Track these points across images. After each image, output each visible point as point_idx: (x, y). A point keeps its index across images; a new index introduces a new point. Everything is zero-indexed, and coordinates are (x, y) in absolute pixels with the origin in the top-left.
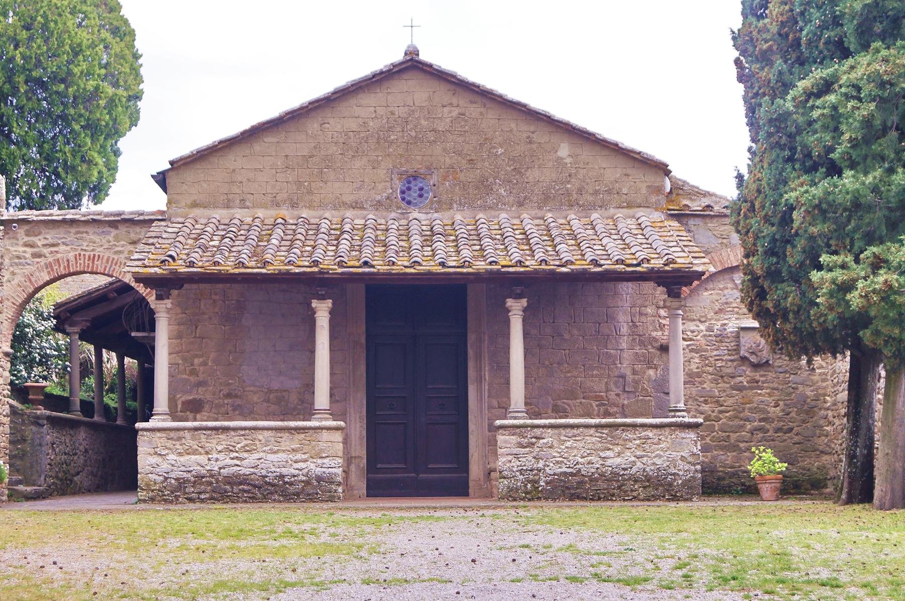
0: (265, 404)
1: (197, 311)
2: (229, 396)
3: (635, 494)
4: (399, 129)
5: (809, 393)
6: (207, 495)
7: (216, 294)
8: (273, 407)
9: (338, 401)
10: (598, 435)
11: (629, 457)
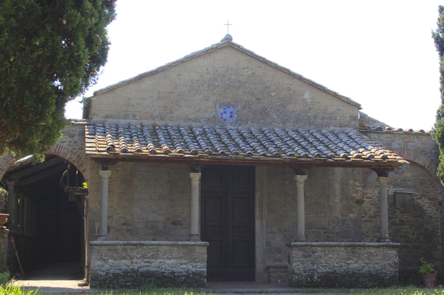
2: (125, 224)
3: (364, 284)
4: (220, 79)
5: (429, 228)
6: (131, 283)
9: (185, 228)
10: (345, 251)
11: (361, 263)
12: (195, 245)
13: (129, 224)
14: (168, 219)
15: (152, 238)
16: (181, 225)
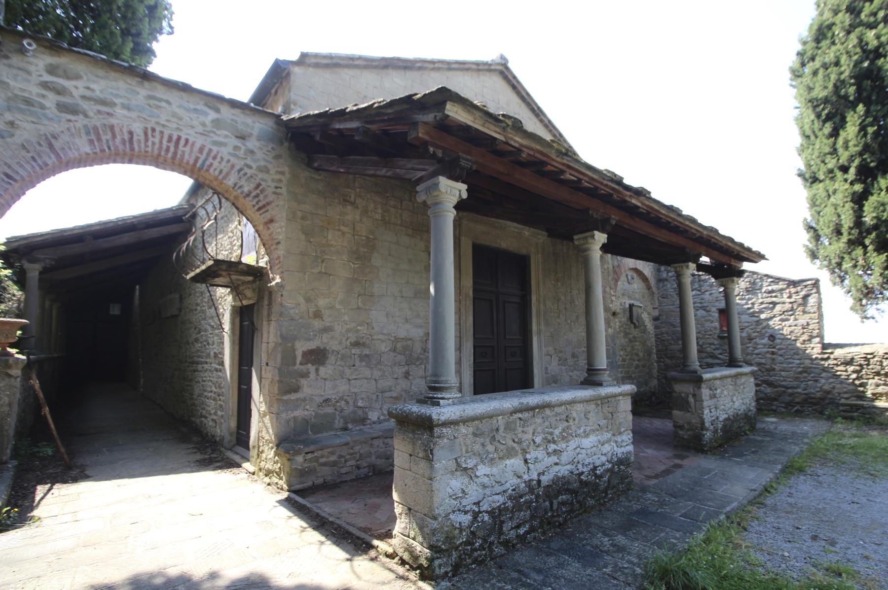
0: (392, 354)
1: (324, 241)
2: (356, 344)
8: (400, 358)
13: (364, 345)
15: (404, 370)
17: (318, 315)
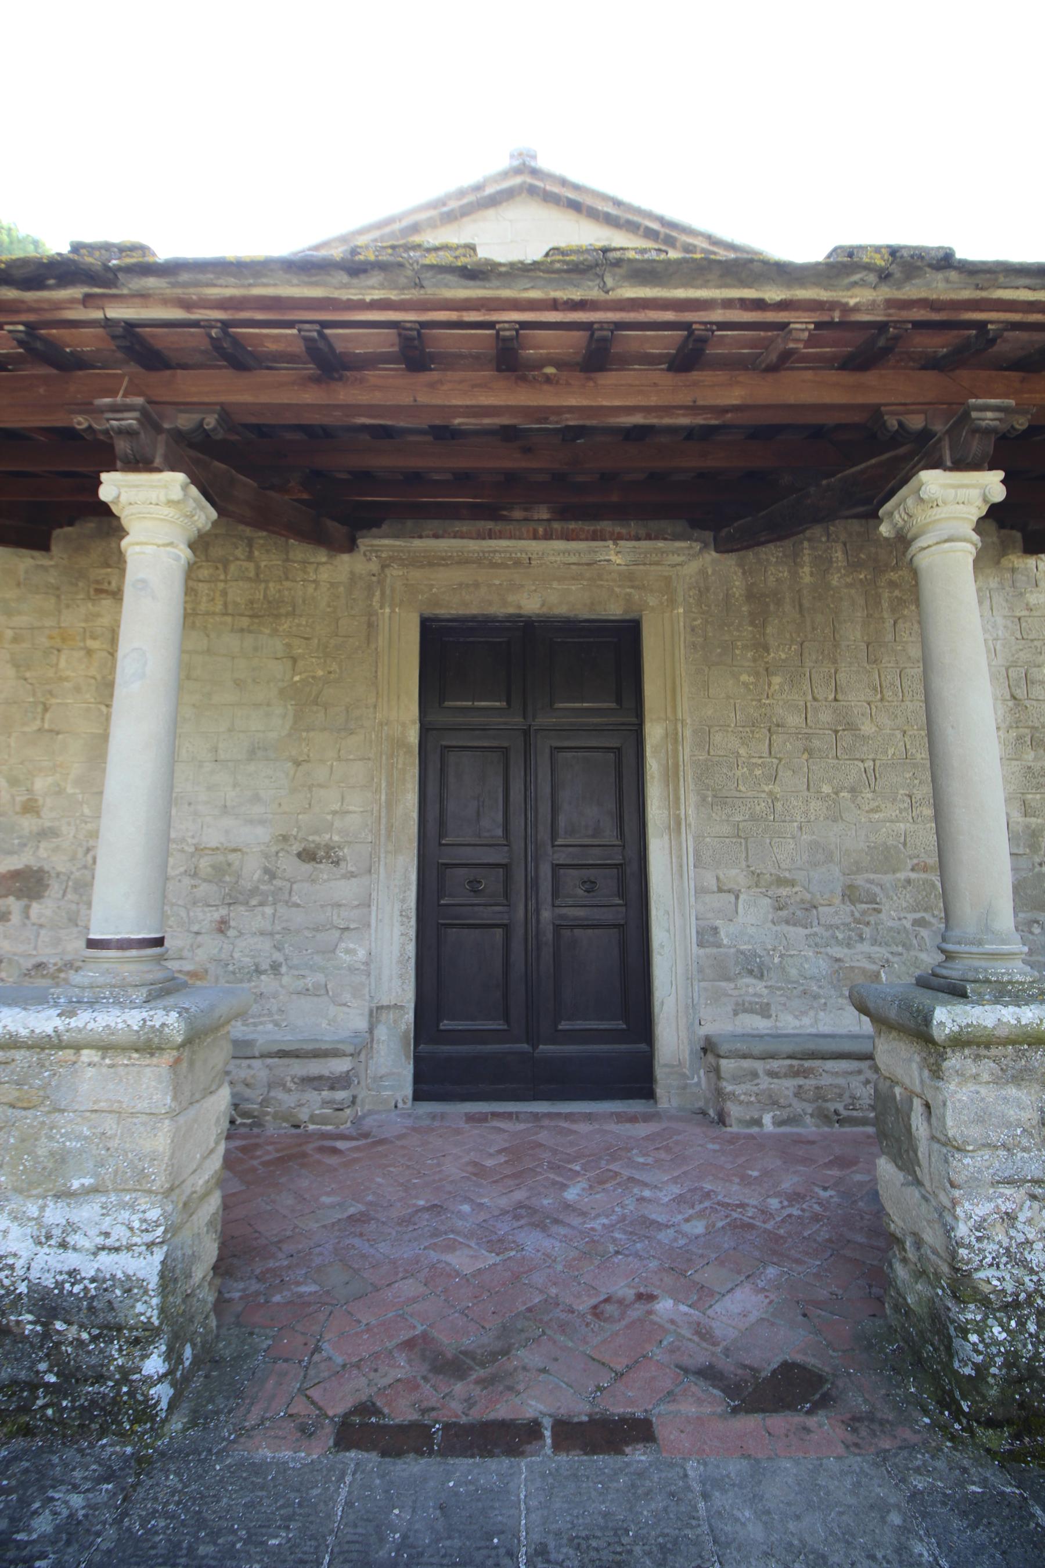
0: (187, 881)
1: (51, 673)
7: (94, 638)
8: (204, 889)
9: (352, 875)
12: (44, 1045)
14: (285, 838)
15: (217, 916)
16: (337, 863)
17: (30, 808)
